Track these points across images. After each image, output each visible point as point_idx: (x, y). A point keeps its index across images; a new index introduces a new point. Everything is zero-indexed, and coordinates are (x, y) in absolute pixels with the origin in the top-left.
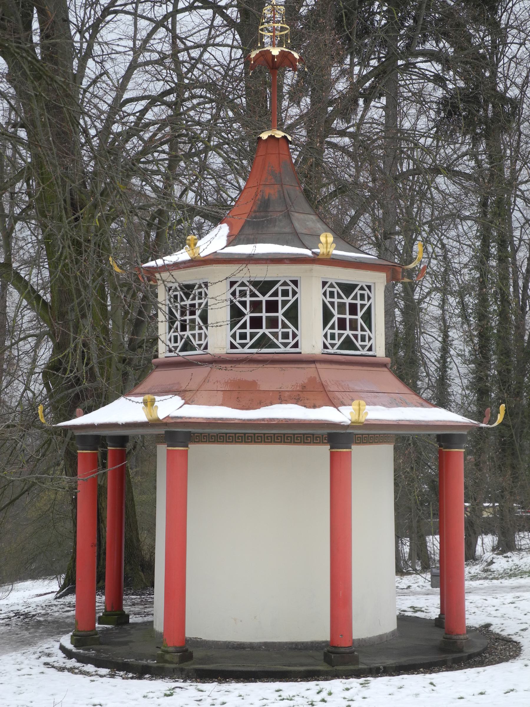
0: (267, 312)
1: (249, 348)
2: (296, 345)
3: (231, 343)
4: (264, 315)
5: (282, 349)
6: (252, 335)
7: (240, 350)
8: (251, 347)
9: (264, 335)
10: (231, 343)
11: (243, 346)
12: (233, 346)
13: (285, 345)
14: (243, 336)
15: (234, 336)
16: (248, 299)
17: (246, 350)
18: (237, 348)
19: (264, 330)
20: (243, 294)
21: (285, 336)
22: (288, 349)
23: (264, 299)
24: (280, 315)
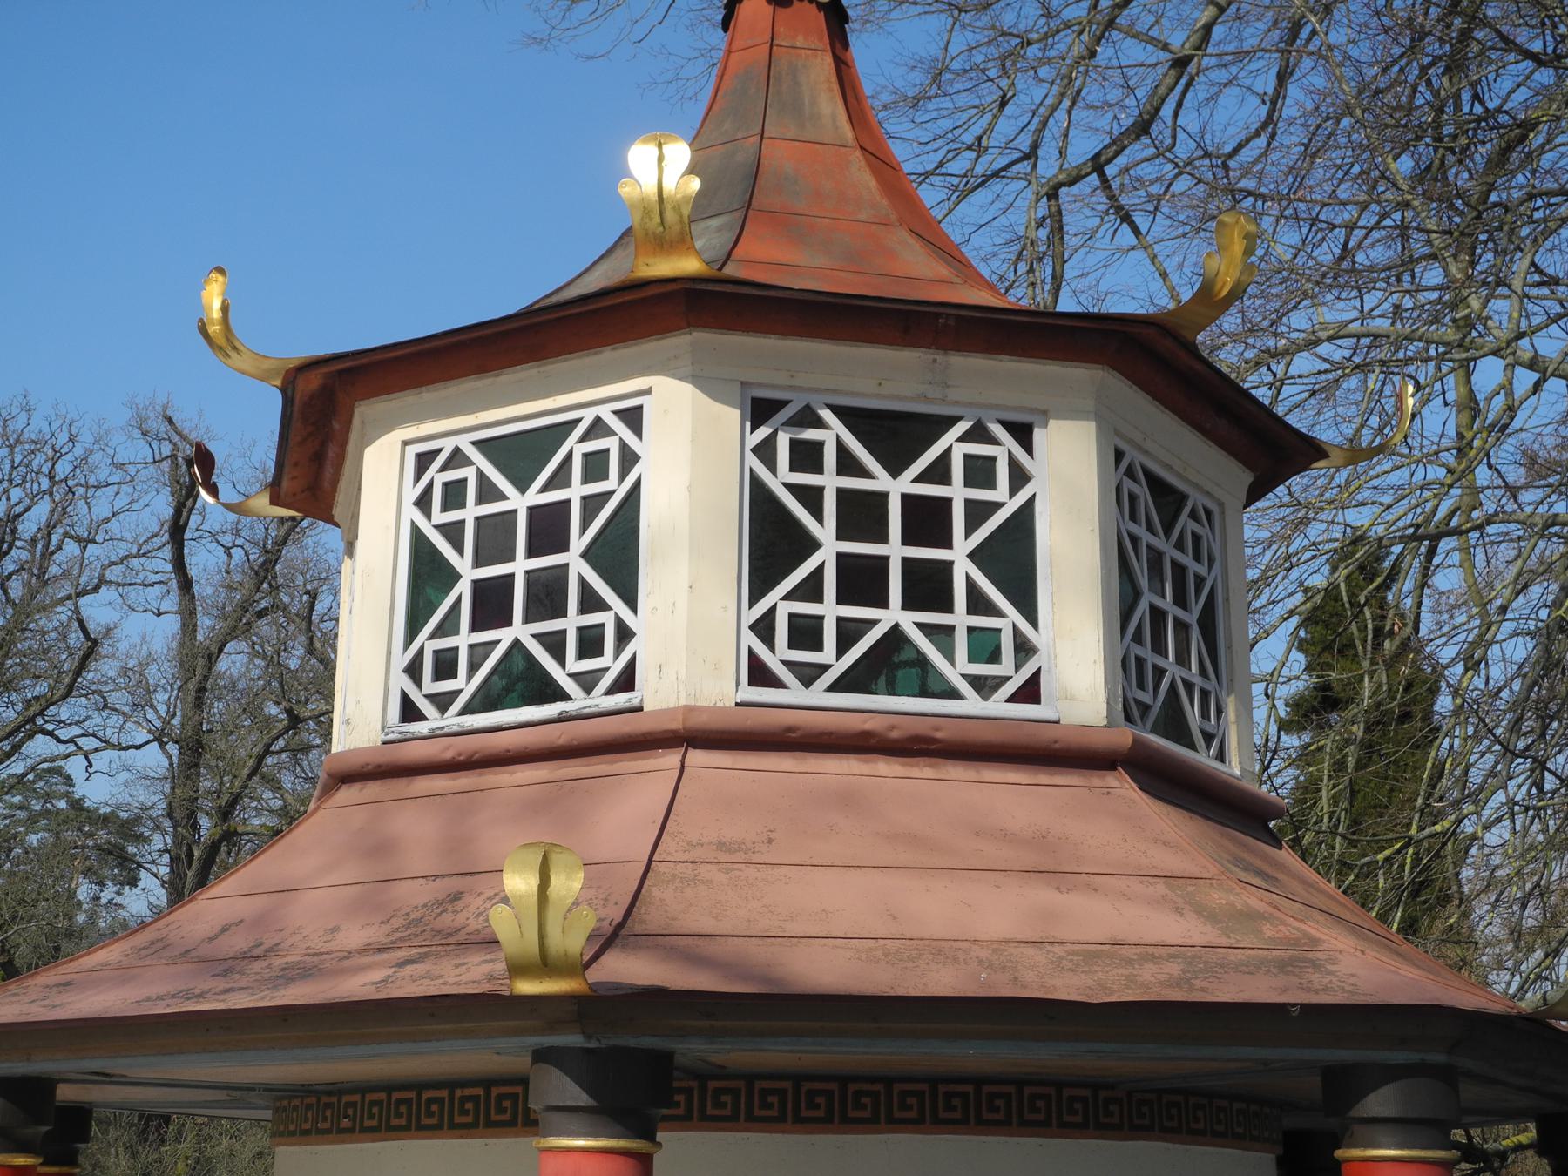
0: (907, 540)
1: (832, 688)
2: (1030, 692)
3: (753, 657)
4: (895, 550)
5: (972, 704)
6: (848, 633)
7: (795, 693)
8: (843, 684)
9: (895, 635)
10: (753, 657)
11: (808, 674)
12: (760, 674)
13: (984, 686)
14: (806, 633)
15: (764, 628)
16: (830, 481)
17: (818, 695)
18: (777, 683)
19: (894, 615)
20: (808, 456)
21: (985, 646)
22: (997, 706)
23: (896, 487)
24: (959, 555)
